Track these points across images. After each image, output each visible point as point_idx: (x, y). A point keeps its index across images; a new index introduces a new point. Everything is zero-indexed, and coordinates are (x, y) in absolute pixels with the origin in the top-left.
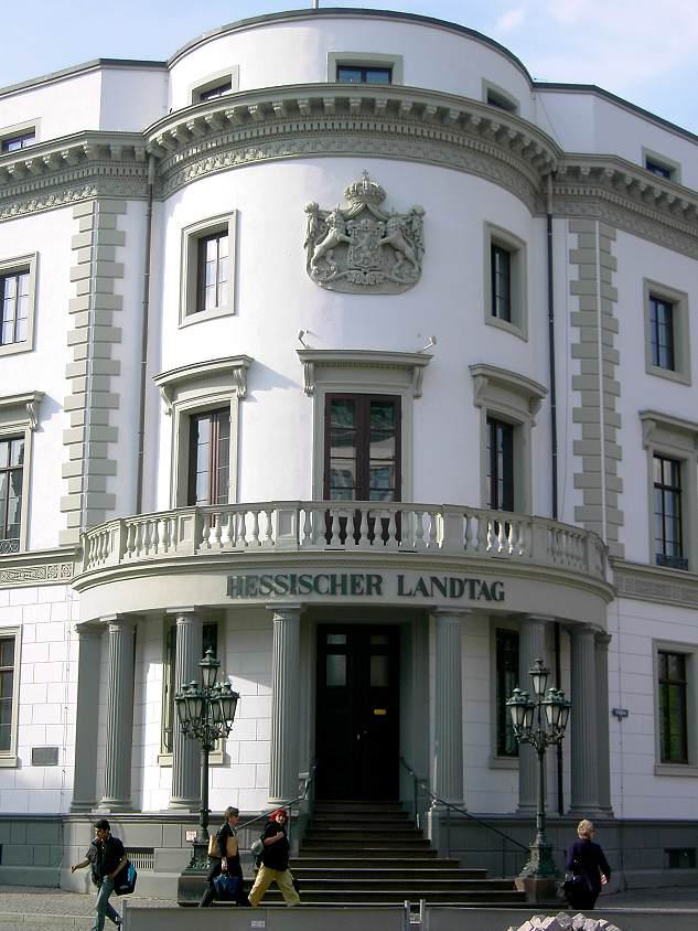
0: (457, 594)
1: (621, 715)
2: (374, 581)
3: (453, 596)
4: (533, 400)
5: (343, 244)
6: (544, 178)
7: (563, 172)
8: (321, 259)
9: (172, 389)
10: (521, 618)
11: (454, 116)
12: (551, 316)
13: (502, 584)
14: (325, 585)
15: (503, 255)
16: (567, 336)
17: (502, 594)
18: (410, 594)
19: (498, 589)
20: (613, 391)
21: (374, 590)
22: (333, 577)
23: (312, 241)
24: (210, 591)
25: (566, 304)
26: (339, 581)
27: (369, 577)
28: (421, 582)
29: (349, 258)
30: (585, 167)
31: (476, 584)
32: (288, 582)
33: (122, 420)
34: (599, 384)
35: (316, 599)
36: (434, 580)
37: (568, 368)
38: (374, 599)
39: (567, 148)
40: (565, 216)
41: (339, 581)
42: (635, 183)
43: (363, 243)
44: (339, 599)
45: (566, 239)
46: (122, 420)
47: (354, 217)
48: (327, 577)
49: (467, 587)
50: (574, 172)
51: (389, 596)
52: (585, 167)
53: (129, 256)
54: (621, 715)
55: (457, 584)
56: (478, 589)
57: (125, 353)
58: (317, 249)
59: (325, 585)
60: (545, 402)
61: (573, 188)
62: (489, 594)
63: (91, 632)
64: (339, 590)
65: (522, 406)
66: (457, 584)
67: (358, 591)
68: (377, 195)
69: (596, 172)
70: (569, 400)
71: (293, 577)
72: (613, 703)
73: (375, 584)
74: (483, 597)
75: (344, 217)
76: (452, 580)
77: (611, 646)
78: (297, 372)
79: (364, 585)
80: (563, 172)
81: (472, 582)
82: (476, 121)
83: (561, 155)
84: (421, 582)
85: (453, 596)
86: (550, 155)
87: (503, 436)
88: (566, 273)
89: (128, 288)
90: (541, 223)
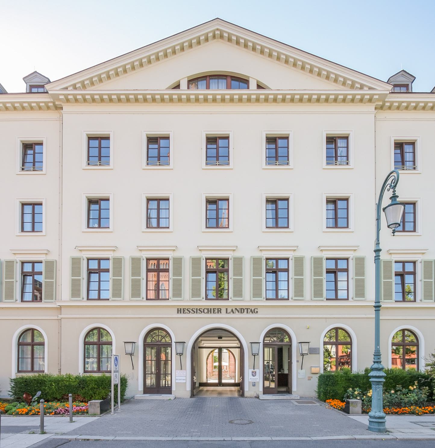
0: (242, 312)
2: (219, 310)
3: (241, 313)
13: (257, 309)
17: (257, 312)
18: (229, 313)
19: (256, 310)
21: (219, 312)
22: (208, 309)
26: (209, 310)
27: (218, 309)
28: (232, 310)
31: (249, 309)
32: (195, 311)
36: (236, 309)
41: (209, 310)
48: (206, 309)
49: (246, 311)
55: (242, 310)
56: (249, 311)
64: (209, 312)
66: (242, 310)
67: (215, 312)
71: (197, 309)
74: (251, 313)
76: (241, 309)
79: (216, 311)
81: (247, 309)
84: (232, 310)
85: (241, 313)
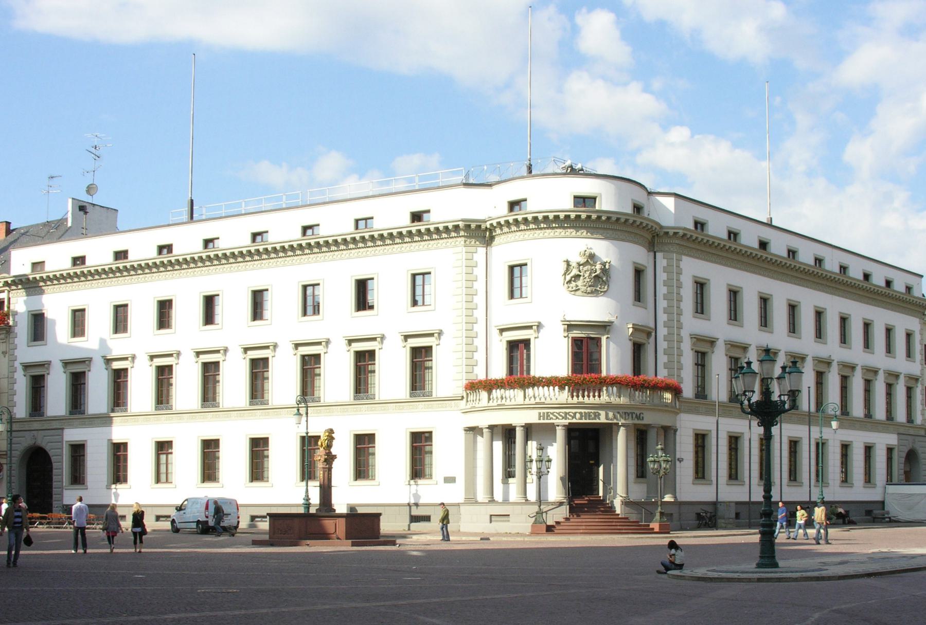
1: (680, 460)
4: (649, 334)
5: (577, 277)
6: (654, 237)
7: (662, 234)
8: (569, 282)
9: (502, 331)
10: (648, 426)
11: (623, 220)
12: (655, 296)
14: (578, 416)
15: (639, 273)
16: (662, 304)
20: (680, 327)
22: (581, 413)
23: (565, 274)
24: (532, 417)
25: (662, 290)
29: (580, 283)
30: (671, 232)
33: (480, 342)
34: (675, 324)
35: (574, 421)
37: (662, 317)
38: (597, 421)
39: (664, 224)
40: (661, 251)
42: (691, 236)
43: (587, 275)
44: (584, 421)
45: (662, 262)
46: (480, 342)
47: (584, 265)
50: (667, 233)
51: (603, 419)
52: (671, 232)
53: (480, 272)
54: (680, 460)
57: (480, 314)
58: (568, 278)
59: (578, 416)
60: (653, 334)
61: (666, 240)
62: (638, 417)
63: (473, 430)
65: (644, 336)
68: (592, 256)
69: (675, 233)
70: (662, 331)
72: (678, 456)
73: (597, 416)
75: (579, 265)
77: (678, 433)
78: (561, 328)
80: (662, 234)
81: (632, 413)
82: (631, 221)
83: (661, 227)
86: (655, 226)
87: (638, 349)
88: (662, 276)
89: (480, 286)
90: (652, 254)
